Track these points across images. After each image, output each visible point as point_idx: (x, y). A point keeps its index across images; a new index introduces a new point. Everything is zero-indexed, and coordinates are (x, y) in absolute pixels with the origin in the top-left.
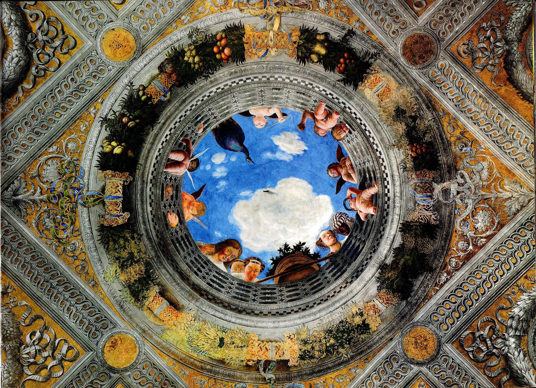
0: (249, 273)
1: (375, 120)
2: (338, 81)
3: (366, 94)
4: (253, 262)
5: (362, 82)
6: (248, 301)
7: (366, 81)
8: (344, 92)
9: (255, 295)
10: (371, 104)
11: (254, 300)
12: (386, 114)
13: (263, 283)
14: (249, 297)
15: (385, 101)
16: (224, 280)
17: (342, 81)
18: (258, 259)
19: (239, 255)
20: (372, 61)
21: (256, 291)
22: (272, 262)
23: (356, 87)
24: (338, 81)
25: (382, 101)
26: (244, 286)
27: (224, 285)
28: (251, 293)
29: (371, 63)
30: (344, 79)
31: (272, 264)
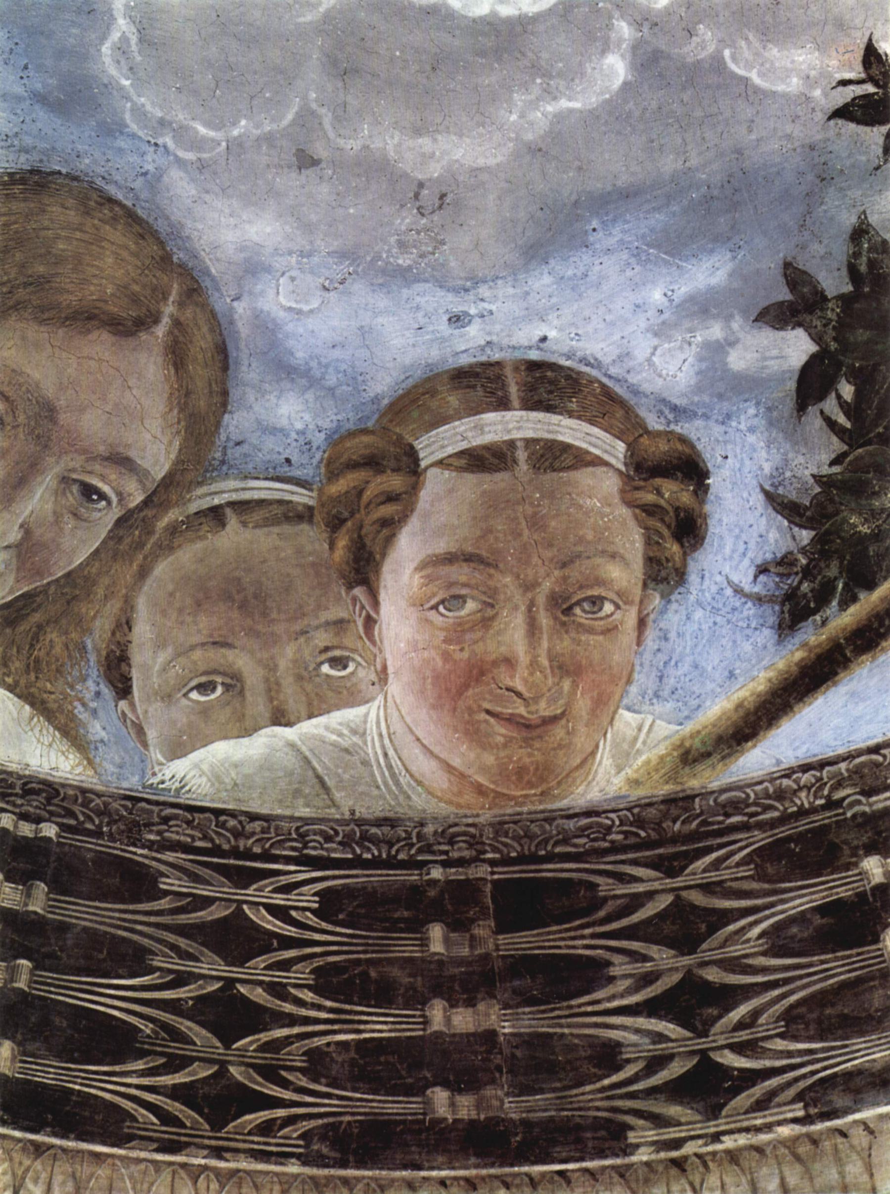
0: (463, 684)
4: (482, 460)
6: (612, 1136)
9: (692, 1002)
11: (708, 1087)
13: (760, 760)
14: (608, 1056)
16: (87, 914)
18: (548, 383)
19: (201, 414)
21: (686, 927)
22: (796, 347)
26: (456, 905)
27: (113, 998)
28: (617, 993)
31: (812, 383)
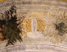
1: (51, 46)
2: (7, 46)
3: (30, 37)
5: (21, 32)
7: (22, 29)
8: (16, 49)
10: (39, 40)
12: (53, 36)
15: (45, 29)
17: (9, 44)
20: (14, 14)
23: (20, 39)
24: (7, 46)
25: (43, 31)
29: (15, 16)
30: (8, 41)
